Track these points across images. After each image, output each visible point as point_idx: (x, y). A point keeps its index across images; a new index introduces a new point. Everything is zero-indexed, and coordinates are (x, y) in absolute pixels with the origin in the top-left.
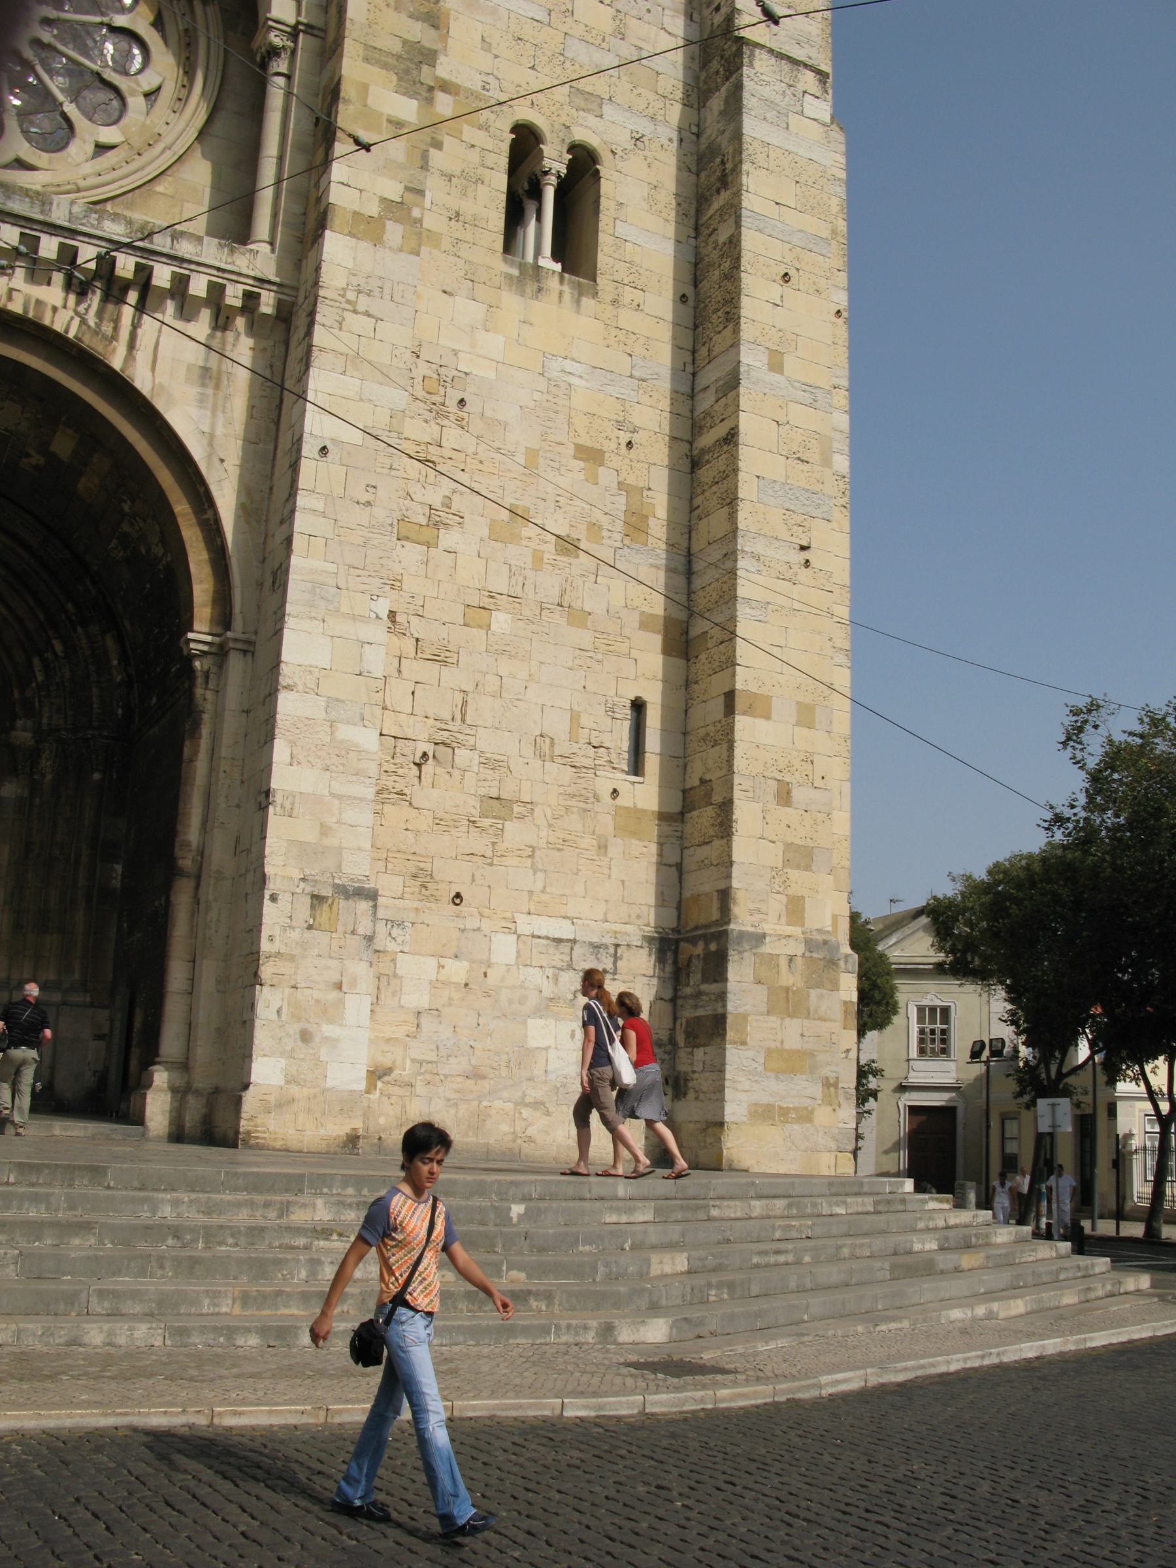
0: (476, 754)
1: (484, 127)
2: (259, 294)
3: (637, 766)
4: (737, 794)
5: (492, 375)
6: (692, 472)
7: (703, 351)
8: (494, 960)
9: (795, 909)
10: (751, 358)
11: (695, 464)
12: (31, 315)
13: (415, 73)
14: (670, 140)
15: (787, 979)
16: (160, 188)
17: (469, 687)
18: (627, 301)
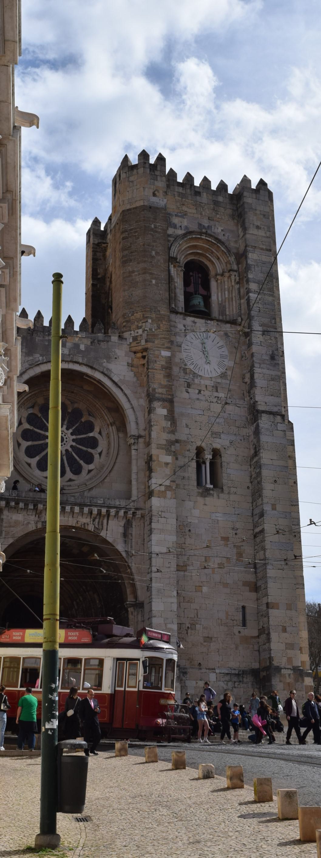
0: (202, 626)
1: (189, 450)
2: (136, 512)
3: (244, 624)
4: (271, 631)
5: (197, 521)
6: (254, 538)
7: (255, 503)
8: (210, 680)
9: (290, 660)
10: (267, 508)
11: (255, 537)
12: (83, 527)
13: (170, 448)
14: (241, 440)
15: (288, 680)
16: (106, 481)
17: (198, 608)
18: (232, 492)
